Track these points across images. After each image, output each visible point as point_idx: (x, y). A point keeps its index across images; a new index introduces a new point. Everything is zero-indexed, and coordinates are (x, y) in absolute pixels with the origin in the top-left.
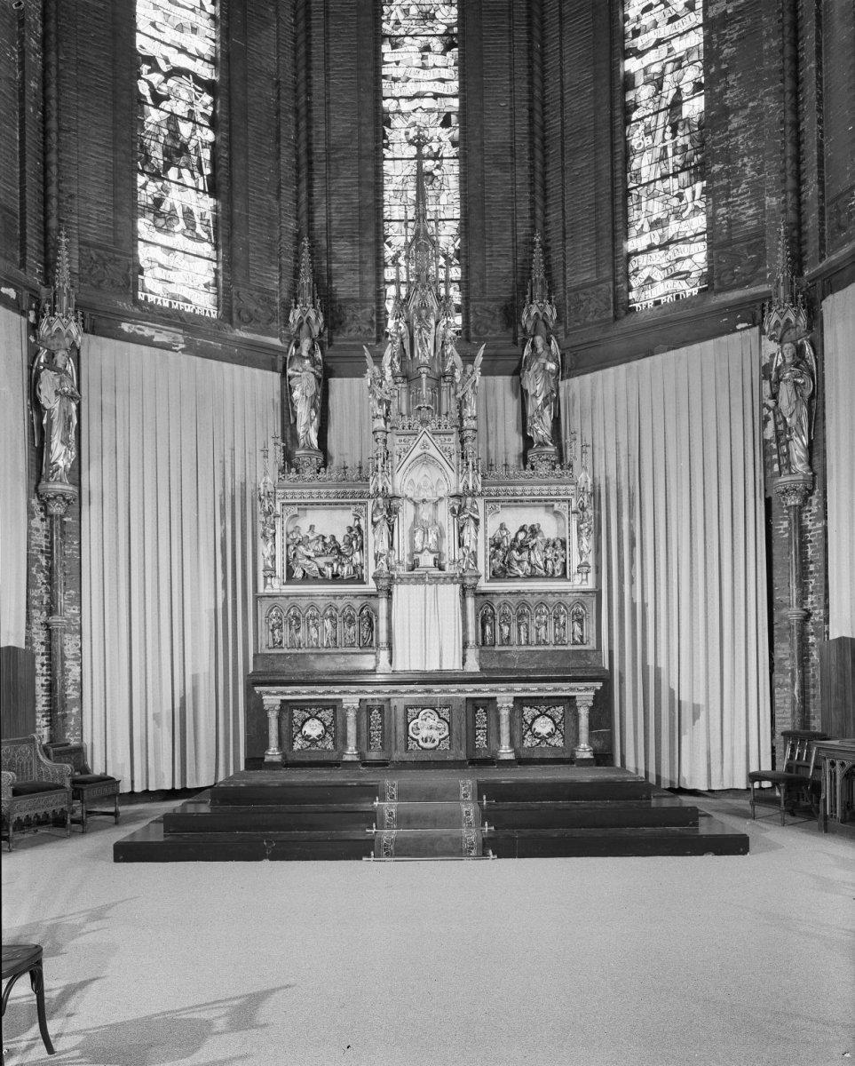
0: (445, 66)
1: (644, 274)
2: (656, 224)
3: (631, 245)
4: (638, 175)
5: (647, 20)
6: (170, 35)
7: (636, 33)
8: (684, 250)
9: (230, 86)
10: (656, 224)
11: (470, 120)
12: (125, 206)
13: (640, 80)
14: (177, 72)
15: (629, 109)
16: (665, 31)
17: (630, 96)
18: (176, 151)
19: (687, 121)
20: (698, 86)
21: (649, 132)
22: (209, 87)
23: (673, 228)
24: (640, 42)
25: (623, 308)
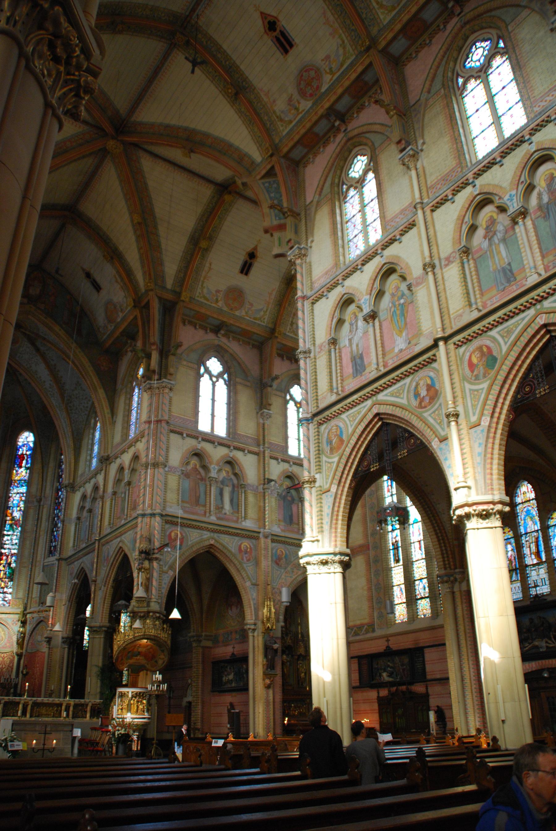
8: (7, 595)
16: (10, 547)
20: (15, 561)
21: (4, 566)
24: (5, 546)
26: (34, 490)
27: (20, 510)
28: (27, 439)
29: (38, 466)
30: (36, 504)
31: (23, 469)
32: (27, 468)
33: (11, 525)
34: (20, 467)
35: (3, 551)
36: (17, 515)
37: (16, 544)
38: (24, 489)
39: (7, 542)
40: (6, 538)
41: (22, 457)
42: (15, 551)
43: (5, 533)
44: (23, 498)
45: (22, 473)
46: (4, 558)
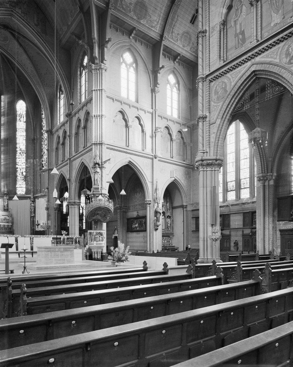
1: (19, 190)
2: (20, 185)
4: (18, 179)
7: (18, 163)
10: (20, 185)
13: (18, 168)
15: (17, 171)
17: (17, 169)
19: (24, 175)
21: (19, 174)
23: (22, 186)
24: (18, 164)
25: (15, 193)
27: (24, 145)
33: (20, 153)
35: (17, 166)
37: (24, 163)
38: (24, 134)
39: (19, 162)
44: (25, 139)
46: (18, 170)
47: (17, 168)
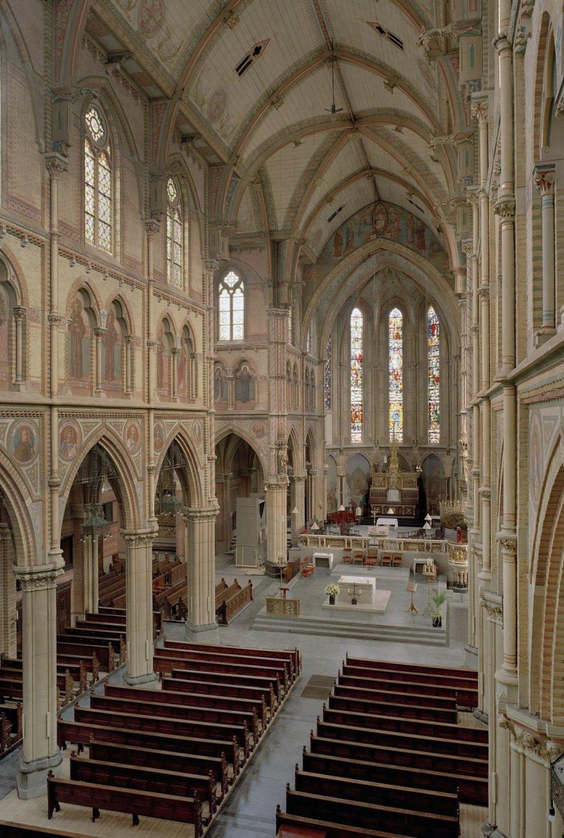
0: (400, 395)
3: (429, 431)
5: (433, 395)
6: (356, 400)
9: (365, 404)
11: (405, 405)
12: (349, 428)
14: (356, 405)
18: (357, 417)
22: (361, 405)
23: (436, 430)
24: (432, 398)
26: (444, 354)
28: (431, 312)
29: (443, 335)
30: (446, 365)
31: (435, 337)
32: (438, 336)
34: (434, 335)
35: (431, 402)
36: (436, 373)
38: (437, 353)
39: (433, 395)
40: (431, 392)
41: (433, 327)
42: (438, 402)
43: (431, 388)
45: (434, 340)
46: (432, 407)
47: (430, 404)
